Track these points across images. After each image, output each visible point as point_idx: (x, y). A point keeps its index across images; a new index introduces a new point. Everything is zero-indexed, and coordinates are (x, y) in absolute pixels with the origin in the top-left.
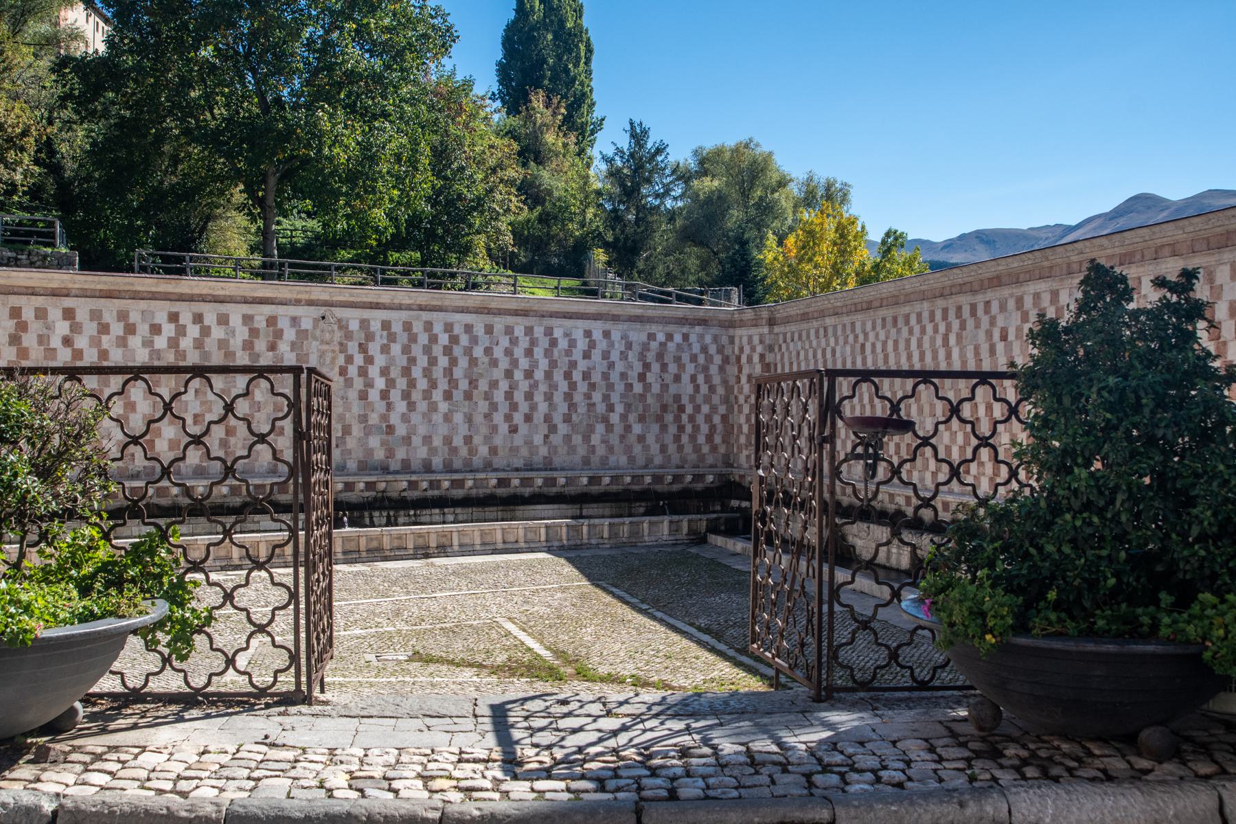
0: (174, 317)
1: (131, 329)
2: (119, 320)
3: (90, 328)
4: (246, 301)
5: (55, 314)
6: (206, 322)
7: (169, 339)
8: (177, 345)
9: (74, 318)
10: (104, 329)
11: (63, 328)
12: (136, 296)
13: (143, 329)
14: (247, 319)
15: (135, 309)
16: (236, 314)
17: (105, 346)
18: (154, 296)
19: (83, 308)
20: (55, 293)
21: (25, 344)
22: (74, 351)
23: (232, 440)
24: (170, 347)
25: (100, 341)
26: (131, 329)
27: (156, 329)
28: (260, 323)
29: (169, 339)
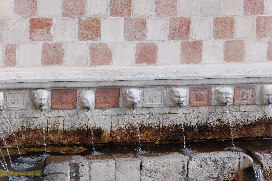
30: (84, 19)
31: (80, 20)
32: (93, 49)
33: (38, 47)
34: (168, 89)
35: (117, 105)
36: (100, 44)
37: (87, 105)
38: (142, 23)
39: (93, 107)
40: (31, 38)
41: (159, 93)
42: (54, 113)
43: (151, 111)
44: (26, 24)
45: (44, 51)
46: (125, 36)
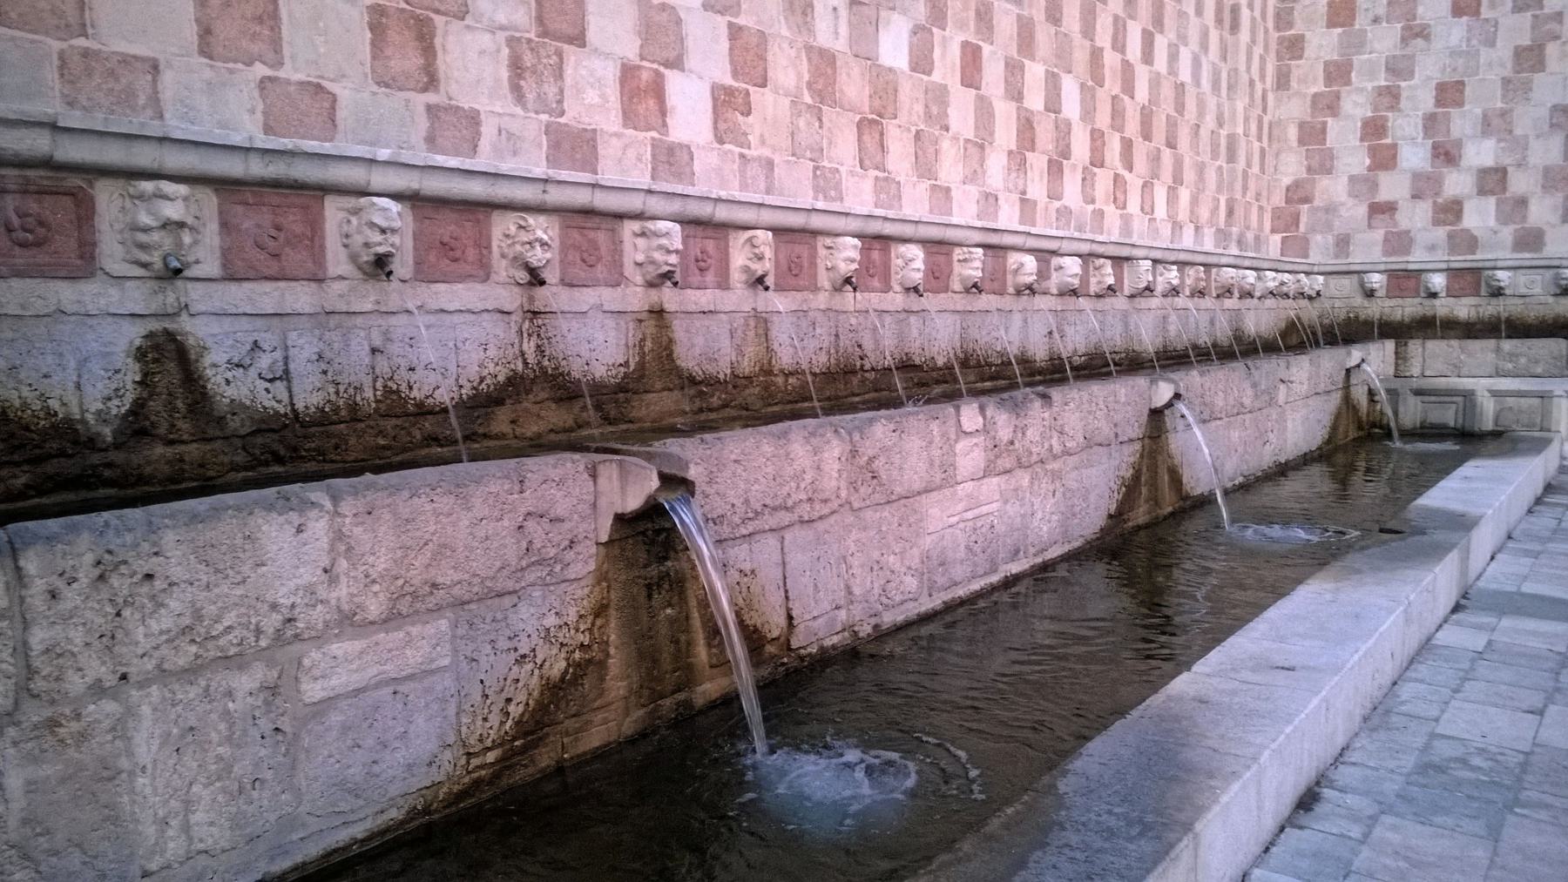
30: (1440, 200)
31: (1435, 202)
32: (1451, 236)
33: (1378, 235)
34: (1552, 272)
35: (1476, 293)
36: (1462, 230)
37: (1433, 290)
38: (1522, 202)
39: (1444, 294)
40: (1370, 226)
41: (1539, 278)
42: (1393, 302)
43: (1527, 300)
44: (1362, 210)
45: (1386, 240)
46: (1497, 219)
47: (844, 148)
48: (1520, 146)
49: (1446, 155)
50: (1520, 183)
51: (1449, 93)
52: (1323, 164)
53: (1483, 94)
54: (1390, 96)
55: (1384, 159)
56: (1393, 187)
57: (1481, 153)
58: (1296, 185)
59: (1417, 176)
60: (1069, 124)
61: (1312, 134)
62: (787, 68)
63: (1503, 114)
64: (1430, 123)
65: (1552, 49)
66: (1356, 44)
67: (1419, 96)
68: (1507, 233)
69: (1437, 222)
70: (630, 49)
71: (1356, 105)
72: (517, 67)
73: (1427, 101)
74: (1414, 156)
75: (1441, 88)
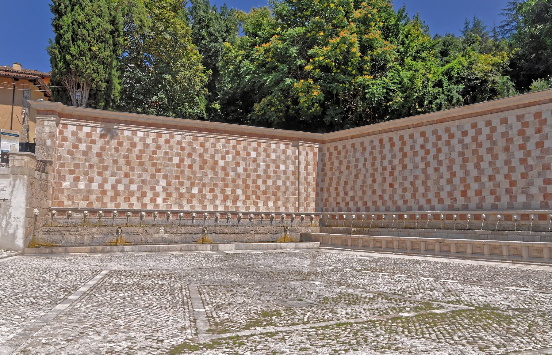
0: (474, 126)
1: (452, 136)
2: (446, 132)
3: (433, 139)
4: (518, 107)
5: (417, 135)
6: (493, 124)
7: (473, 137)
8: (477, 140)
9: (425, 136)
10: (439, 138)
11: (420, 141)
12: (453, 119)
13: (458, 135)
14: (519, 118)
15: (453, 126)
16: (512, 117)
17: (439, 146)
18: (463, 117)
19: (428, 130)
20: (417, 126)
21: (405, 151)
22: (425, 150)
23: (514, 189)
24: (473, 141)
25: (437, 144)
26: (452, 136)
27: (465, 133)
28: (529, 118)
29: (473, 137)
32: (348, 208)
38: (357, 202)
47: (184, 202)
48: (355, 192)
49: (346, 194)
50: (357, 199)
51: (346, 183)
52: (330, 195)
53: (351, 183)
54: (338, 183)
55: (338, 194)
56: (339, 199)
57: (351, 193)
58: (326, 199)
59: (343, 198)
60: (238, 196)
61: (328, 190)
62: (175, 195)
63: (354, 186)
64: (344, 188)
65: (359, 175)
66: (333, 174)
67: (342, 183)
68: (355, 208)
69: (346, 206)
70: (152, 196)
71: (334, 185)
72: (138, 199)
73: (343, 183)
74: (342, 194)
75: (345, 182)
